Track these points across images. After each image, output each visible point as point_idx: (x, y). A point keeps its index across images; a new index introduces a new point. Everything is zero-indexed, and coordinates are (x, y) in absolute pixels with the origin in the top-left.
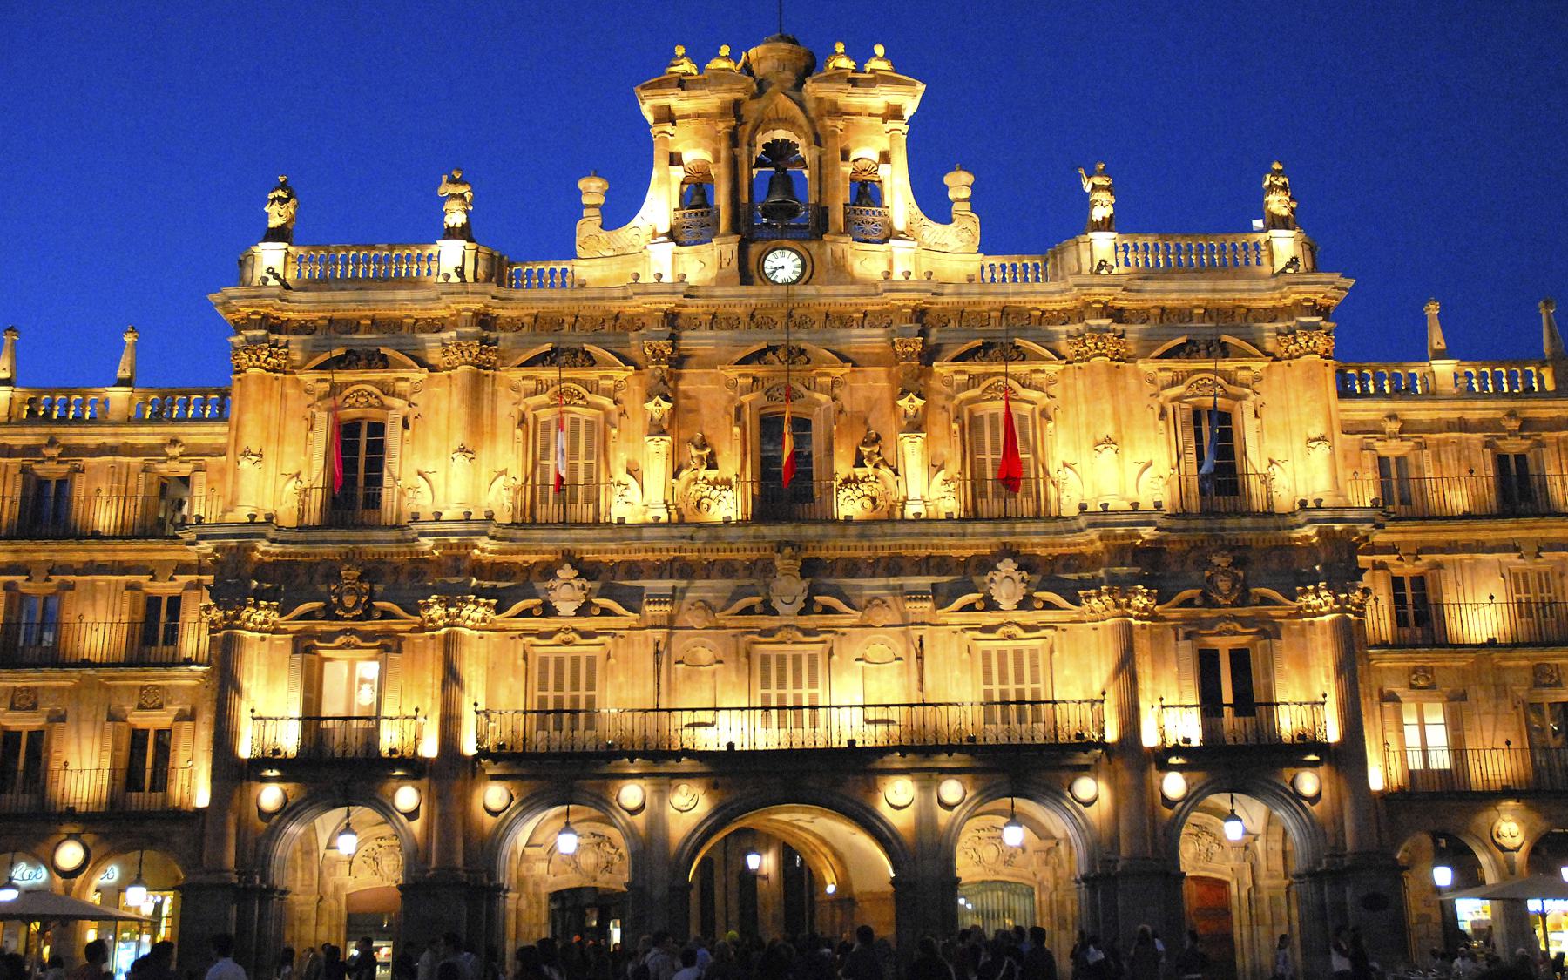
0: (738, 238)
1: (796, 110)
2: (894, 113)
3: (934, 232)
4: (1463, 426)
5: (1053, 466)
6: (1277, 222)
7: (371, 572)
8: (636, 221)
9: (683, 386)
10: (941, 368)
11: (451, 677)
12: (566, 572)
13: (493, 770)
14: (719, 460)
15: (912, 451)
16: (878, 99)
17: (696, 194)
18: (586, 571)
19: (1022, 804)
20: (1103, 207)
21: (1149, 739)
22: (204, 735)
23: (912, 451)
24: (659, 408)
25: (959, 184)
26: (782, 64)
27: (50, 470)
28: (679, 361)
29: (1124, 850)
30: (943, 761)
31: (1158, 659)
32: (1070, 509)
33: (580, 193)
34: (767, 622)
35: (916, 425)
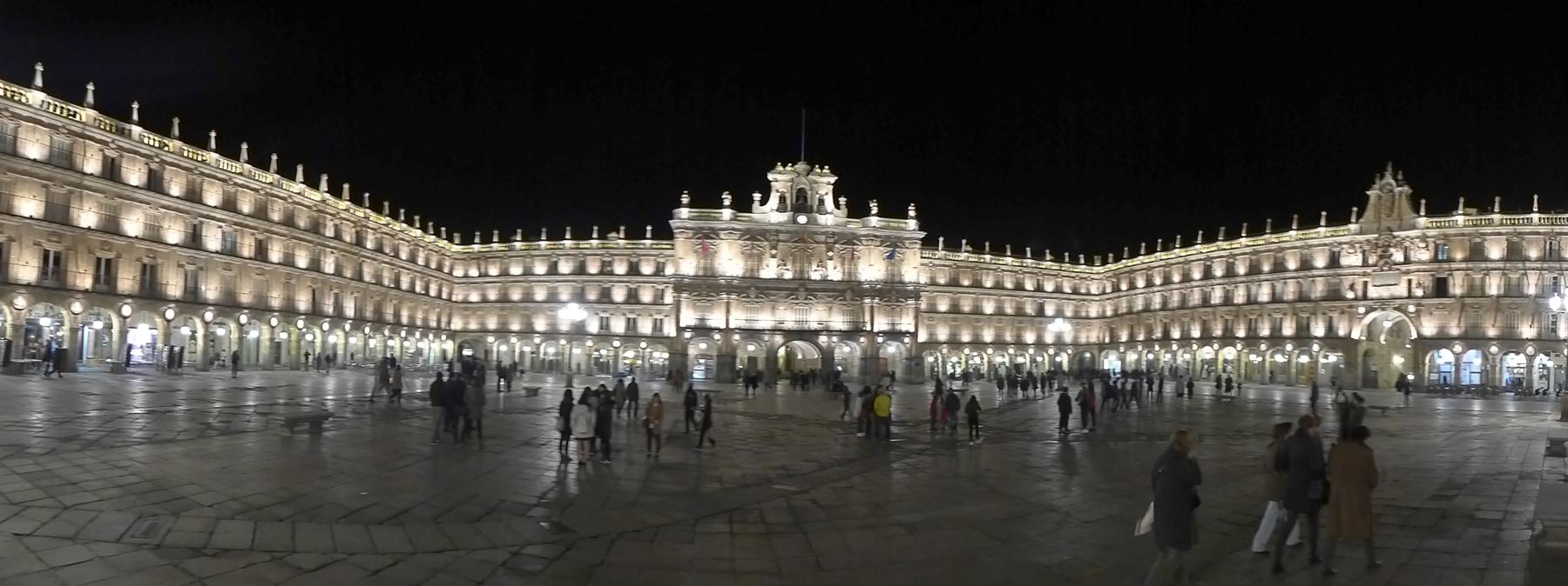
0: (792, 213)
1: (806, 181)
2: (829, 183)
3: (837, 210)
4: (944, 266)
5: (860, 270)
6: (912, 218)
7: (709, 286)
8: (768, 204)
9: (779, 247)
10: (837, 246)
11: (728, 312)
12: (753, 289)
13: (737, 331)
14: (788, 263)
15: (830, 264)
16: (826, 180)
17: (782, 199)
18: (757, 288)
19: (848, 342)
20: (875, 210)
21: (875, 330)
22: (673, 321)
23: (830, 264)
24: (774, 252)
25: (842, 200)
26: (804, 170)
27: (634, 260)
28: (779, 241)
29: (869, 353)
30: (834, 333)
31: (879, 313)
32: (863, 280)
33: (752, 197)
34: (797, 301)
35: (831, 259)
